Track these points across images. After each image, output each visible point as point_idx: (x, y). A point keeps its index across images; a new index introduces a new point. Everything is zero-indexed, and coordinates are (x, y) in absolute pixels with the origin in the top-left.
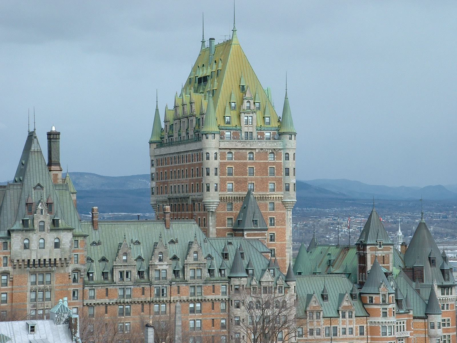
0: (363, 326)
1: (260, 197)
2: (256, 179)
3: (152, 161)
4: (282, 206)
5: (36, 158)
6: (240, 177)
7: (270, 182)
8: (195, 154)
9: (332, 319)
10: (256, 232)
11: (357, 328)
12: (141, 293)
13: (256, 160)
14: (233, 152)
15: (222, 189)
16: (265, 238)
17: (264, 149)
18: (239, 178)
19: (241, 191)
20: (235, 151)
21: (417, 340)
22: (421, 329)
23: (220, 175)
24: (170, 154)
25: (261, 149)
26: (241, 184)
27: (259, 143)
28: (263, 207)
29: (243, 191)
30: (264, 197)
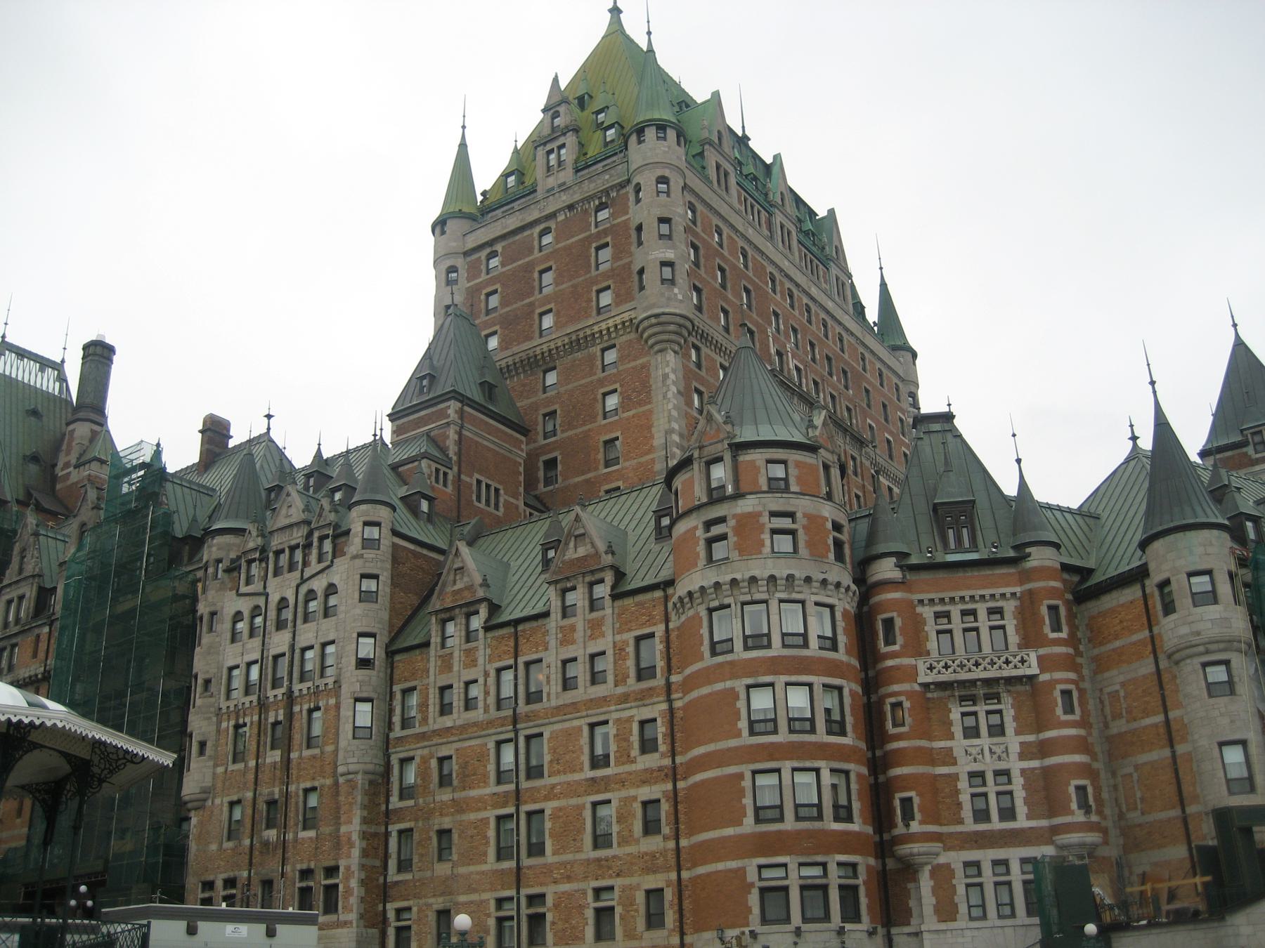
0: (652, 635)
1: (571, 343)
6: (515, 306)
9: (520, 628)
10: (423, 413)
11: (622, 650)
12: (31, 654)
16: (448, 424)
17: (577, 202)
19: (518, 344)
20: (503, 244)
21: (1125, 697)
22: (1135, 638)
25: (571, 207)
27: (562, 193)
28: (583, 367)
29: (524, 342)
30: (581, 335)
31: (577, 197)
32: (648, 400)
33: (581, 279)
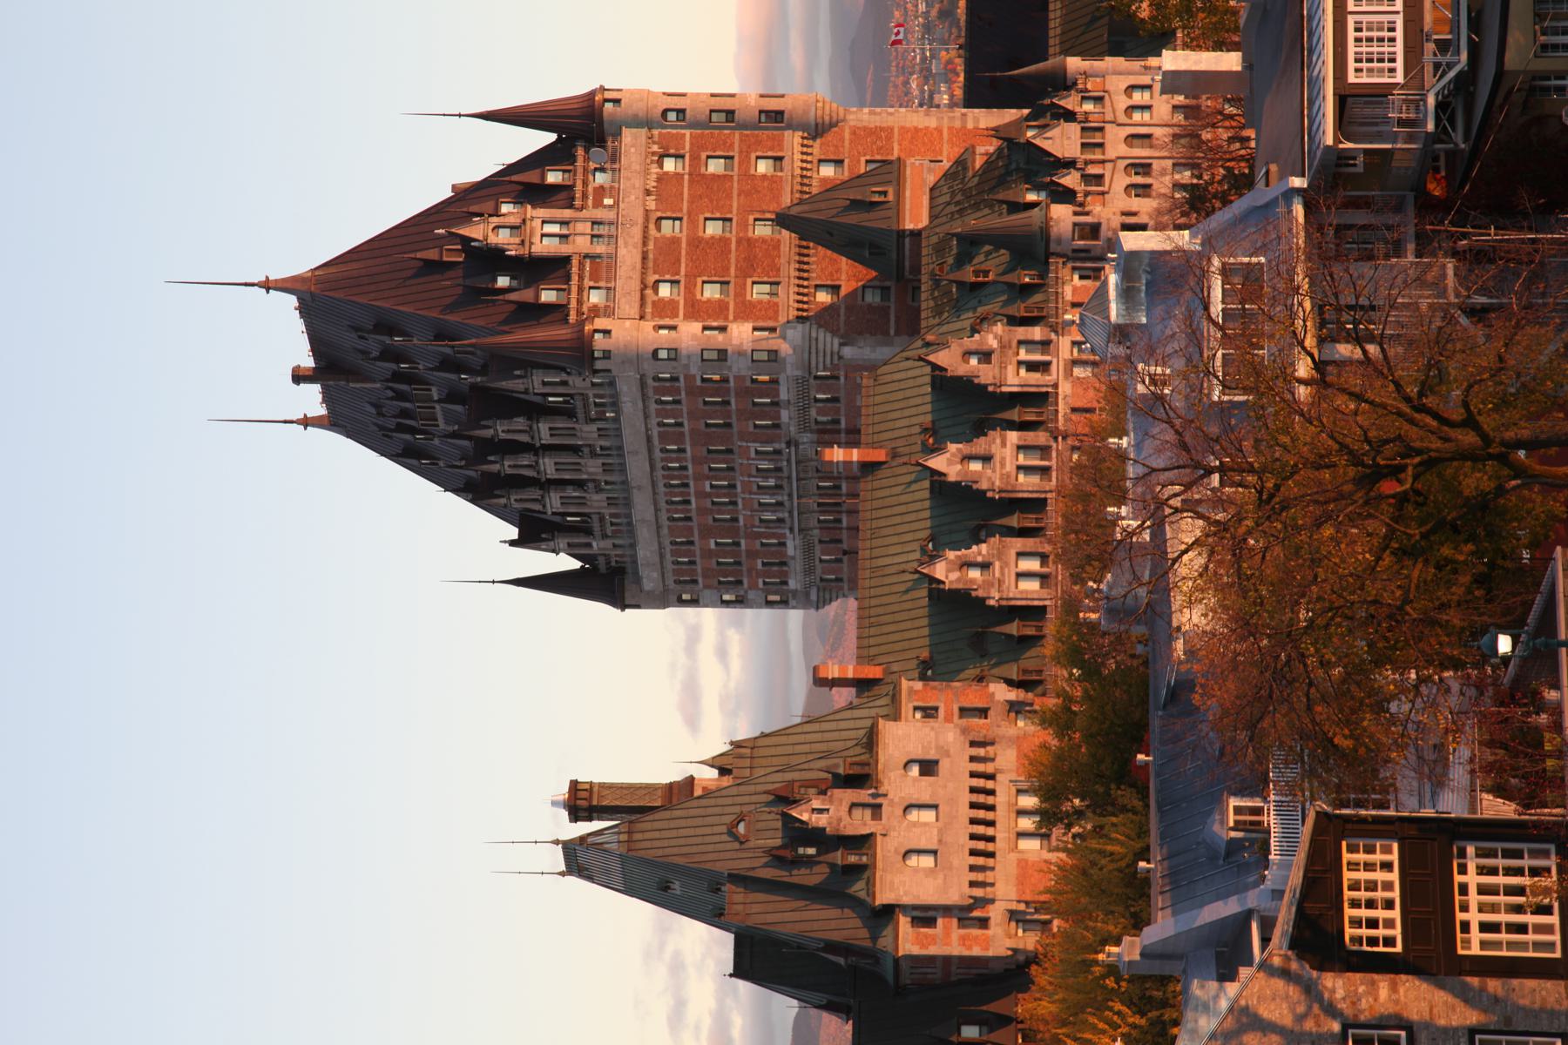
2: (744, 211)
3: (682, 603)
4: (829, 137)
5: (648, 835)
6: (733, 261)
7: (752, 172)
8: (663, 460)
13: (681, 210)
14: (652, 278)
15: (770, 313)
18: (737, 261)
20: (650, 271)
23: (726, 318)
24: (659, 527)
25: (648, 193)
26: (755, 257)
30: (799, 188)
31: (638, 183)
32: (892, 129)
33: (735, 185)
